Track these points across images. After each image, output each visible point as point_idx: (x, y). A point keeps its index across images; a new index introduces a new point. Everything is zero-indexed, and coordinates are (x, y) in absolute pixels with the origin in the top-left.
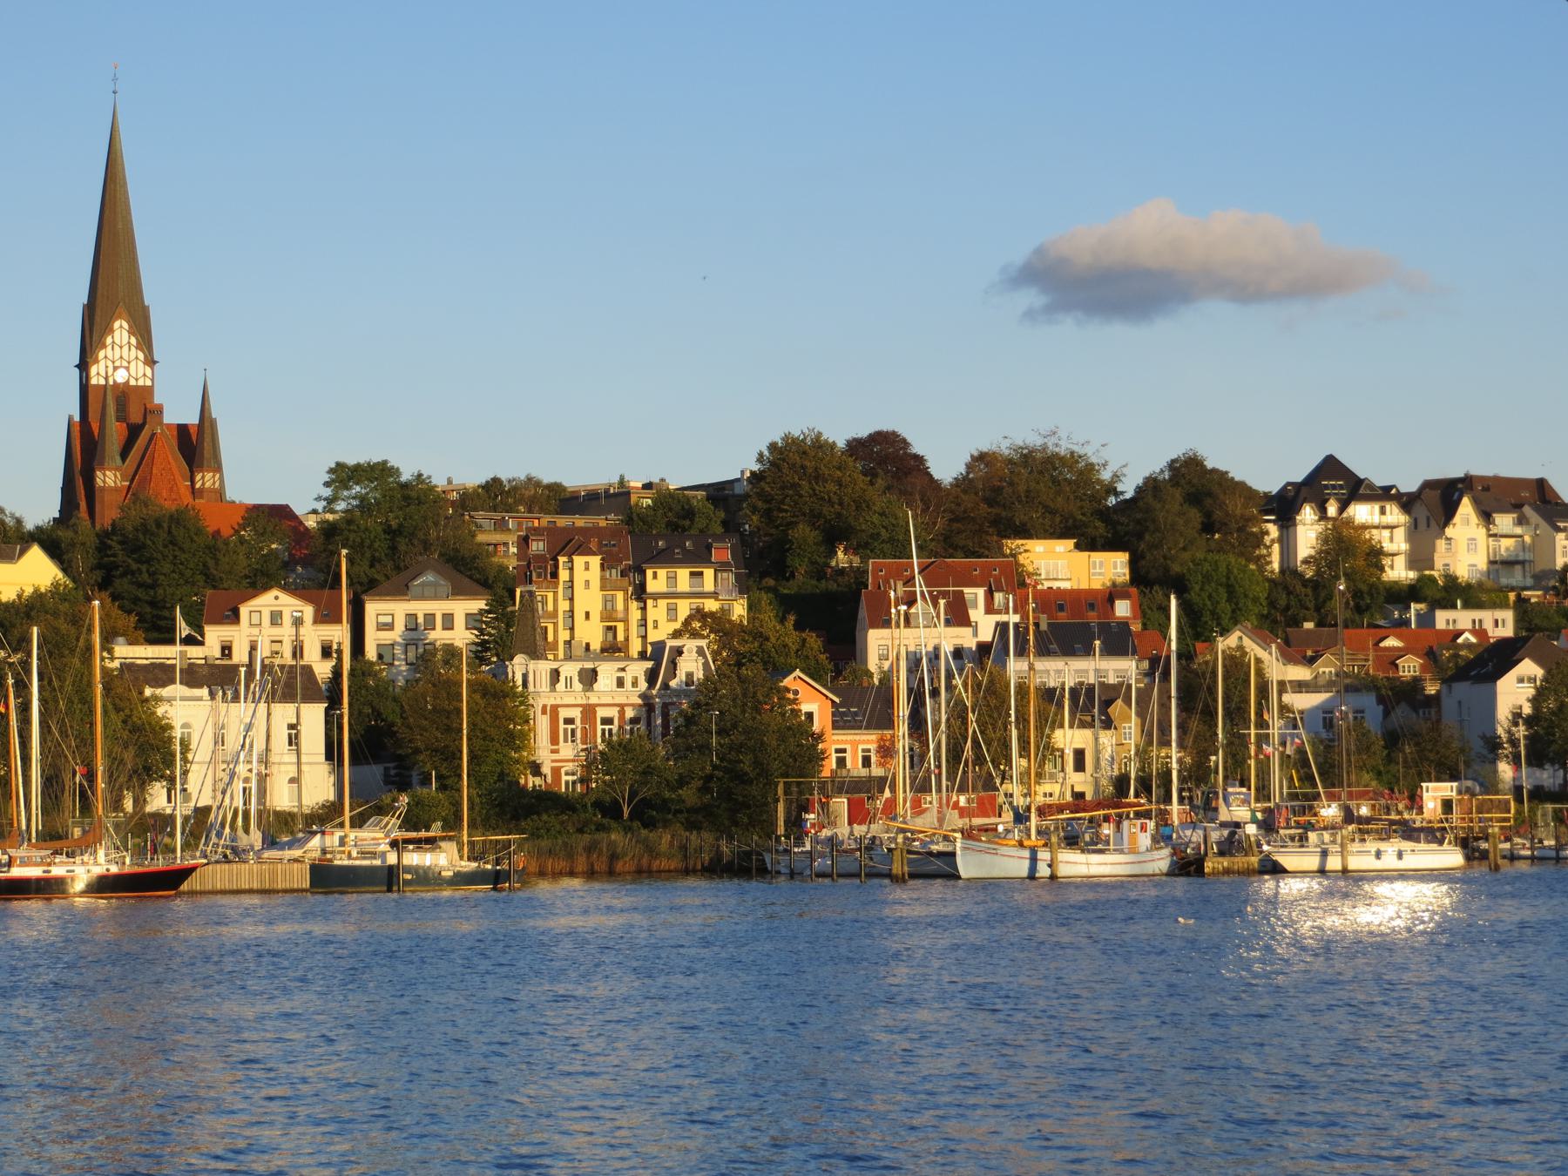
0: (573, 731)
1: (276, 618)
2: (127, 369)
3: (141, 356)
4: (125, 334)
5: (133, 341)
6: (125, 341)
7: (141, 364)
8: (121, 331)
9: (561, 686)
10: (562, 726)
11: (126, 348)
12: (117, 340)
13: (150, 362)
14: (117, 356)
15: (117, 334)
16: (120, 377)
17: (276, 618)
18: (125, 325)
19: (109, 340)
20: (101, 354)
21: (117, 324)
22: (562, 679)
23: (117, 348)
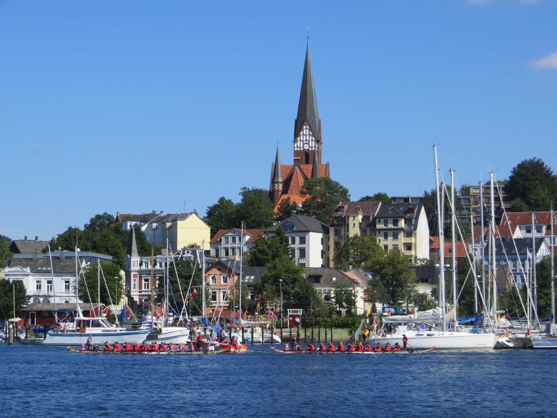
0: (148, 284)
1: (234, 241)
2: (308, 144)
3: (314, 139)
4: (308, 131)
5: (311, 133)
6: (308, 133)
7: (313, 142)
8: (306, 130)
9: (143, 267)
10: (143, 282)
11: (308, 137)
12: (305, 133)
13: (318, 141)
14: (305, 139)
15: (305, 131)
16: (306, 147)
17: (234, 241)
18: (308, 127)
19: (302, 133)
20: (299, 139)
21: (305, 127)
22: (144, 264)
23: (304, 137)
